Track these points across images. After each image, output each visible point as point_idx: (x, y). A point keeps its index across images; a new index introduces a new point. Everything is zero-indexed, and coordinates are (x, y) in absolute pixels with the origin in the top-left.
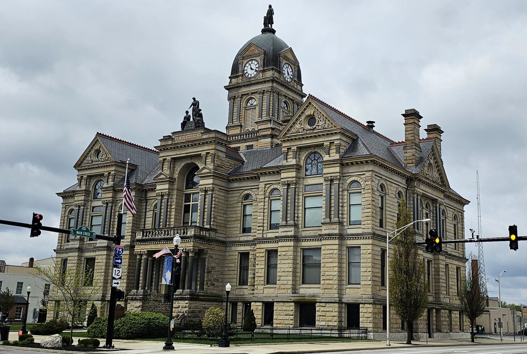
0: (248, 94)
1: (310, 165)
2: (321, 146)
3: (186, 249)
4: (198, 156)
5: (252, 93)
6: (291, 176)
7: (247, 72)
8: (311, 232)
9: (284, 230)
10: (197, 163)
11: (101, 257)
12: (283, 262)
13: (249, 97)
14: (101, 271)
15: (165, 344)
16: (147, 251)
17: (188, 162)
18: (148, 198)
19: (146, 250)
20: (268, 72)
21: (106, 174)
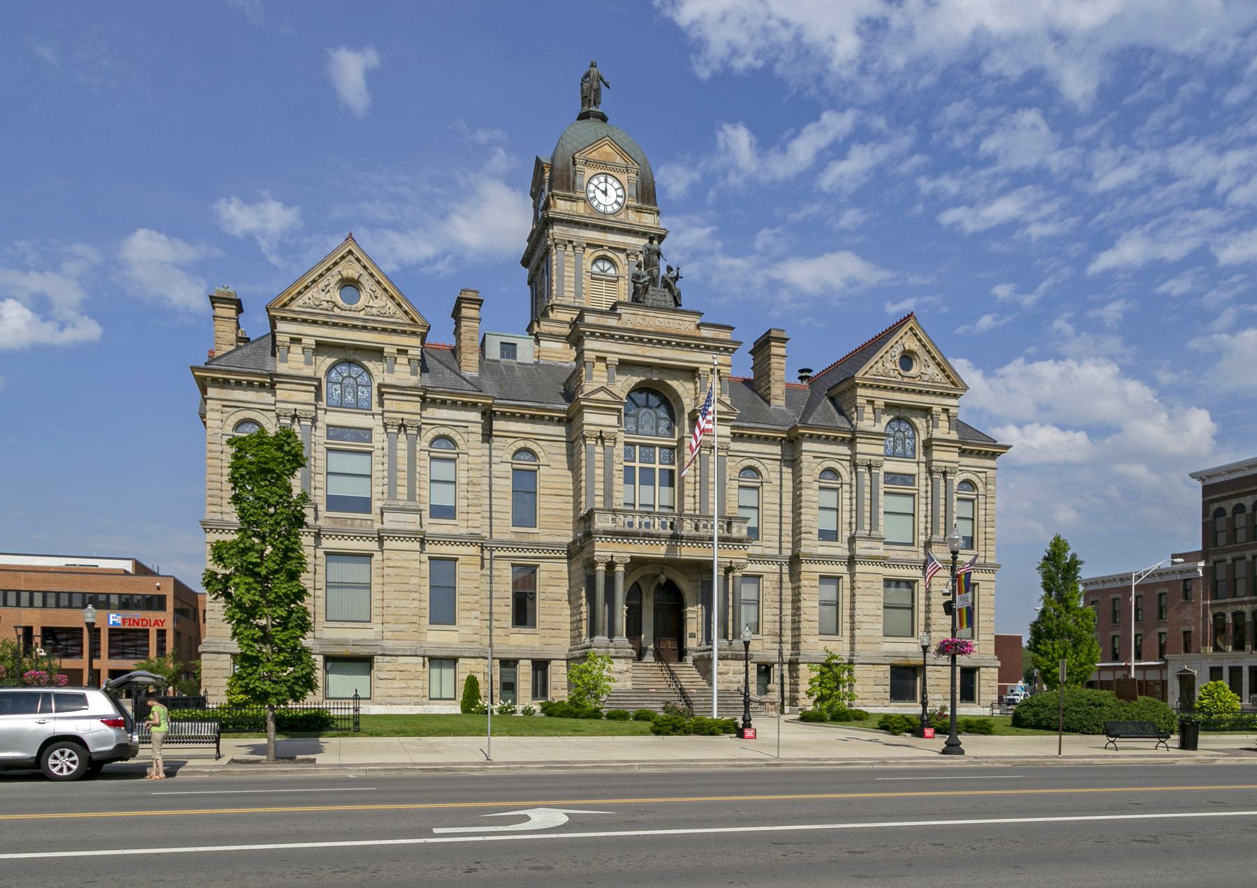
0: (602, 246)
1: (892, 439)
2: (926, 411)
3: (731, 562)
4: (691, 373)
5: (610, 248)
6: (875, 452)
7: (595, 197)
8: (900, 553)
9: (866, 546)
10: (674, 384)
11: (404, 555)
12: (866, 598)
13: (601, 253)
14: (407, 587)
15: (946, 743)
16: (631, 558)
17: (649, 376)
18: (494, 433)
19: (629, 555)
20: (646, 215)
21: (387, 350)
